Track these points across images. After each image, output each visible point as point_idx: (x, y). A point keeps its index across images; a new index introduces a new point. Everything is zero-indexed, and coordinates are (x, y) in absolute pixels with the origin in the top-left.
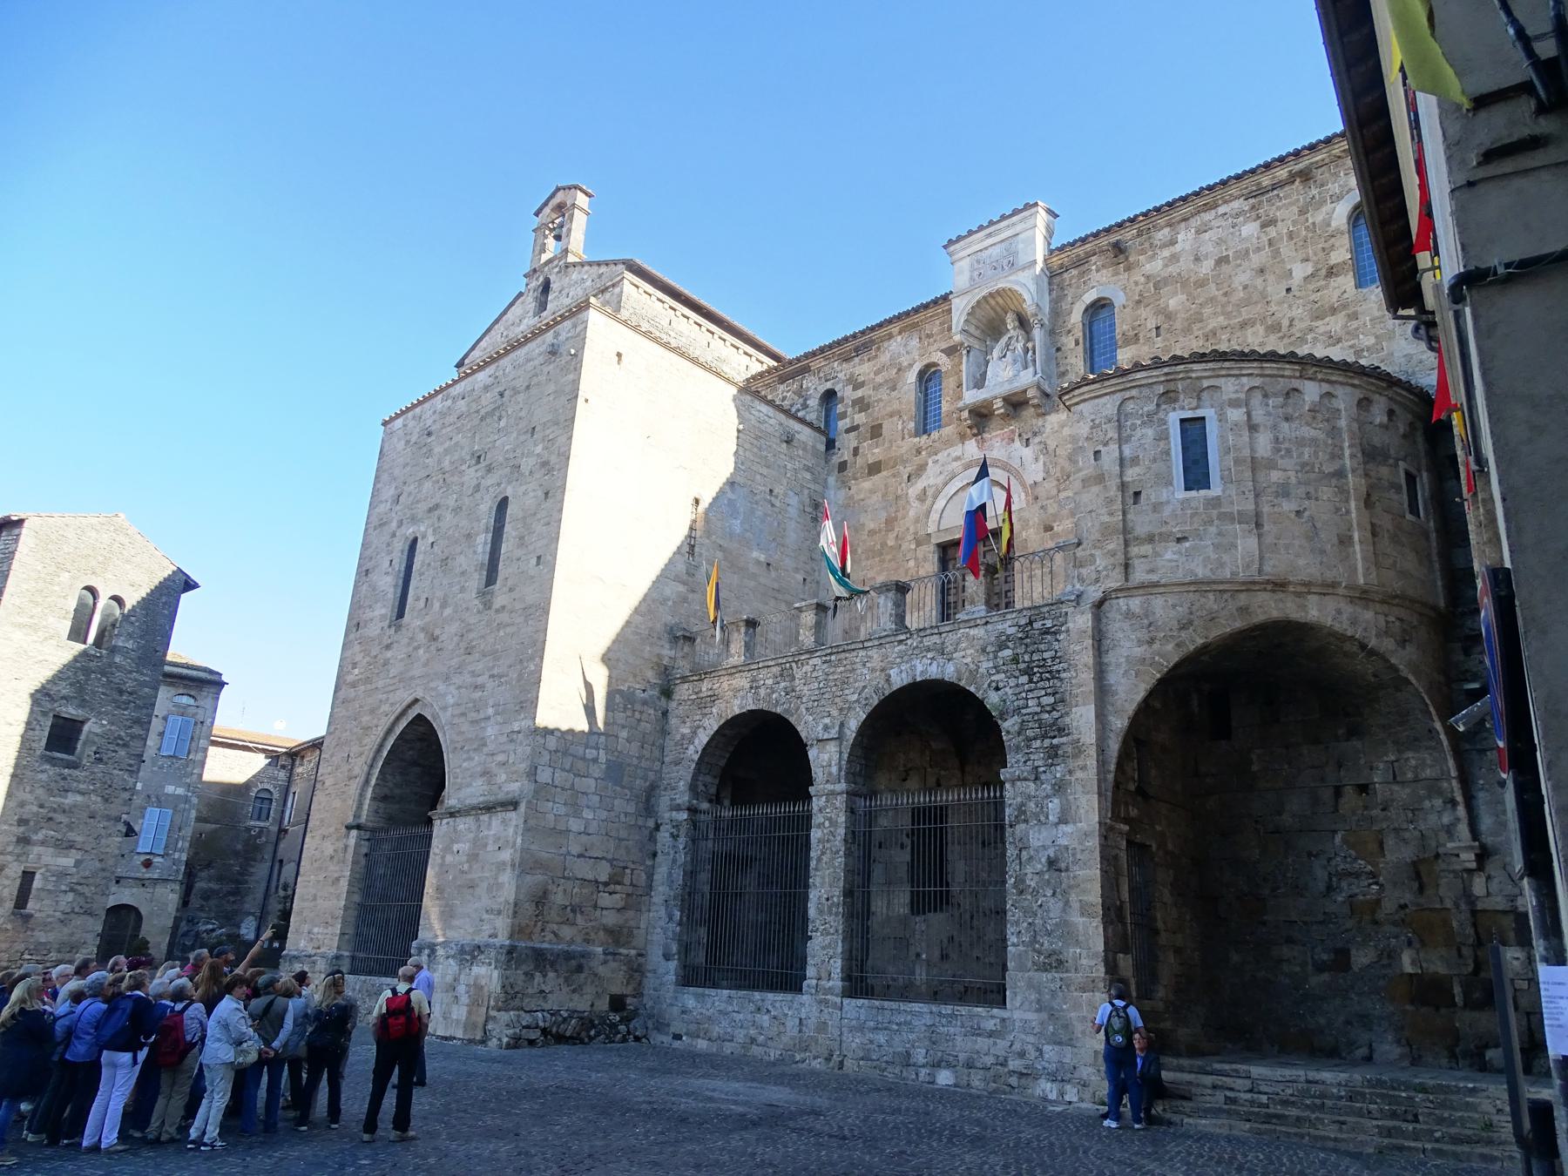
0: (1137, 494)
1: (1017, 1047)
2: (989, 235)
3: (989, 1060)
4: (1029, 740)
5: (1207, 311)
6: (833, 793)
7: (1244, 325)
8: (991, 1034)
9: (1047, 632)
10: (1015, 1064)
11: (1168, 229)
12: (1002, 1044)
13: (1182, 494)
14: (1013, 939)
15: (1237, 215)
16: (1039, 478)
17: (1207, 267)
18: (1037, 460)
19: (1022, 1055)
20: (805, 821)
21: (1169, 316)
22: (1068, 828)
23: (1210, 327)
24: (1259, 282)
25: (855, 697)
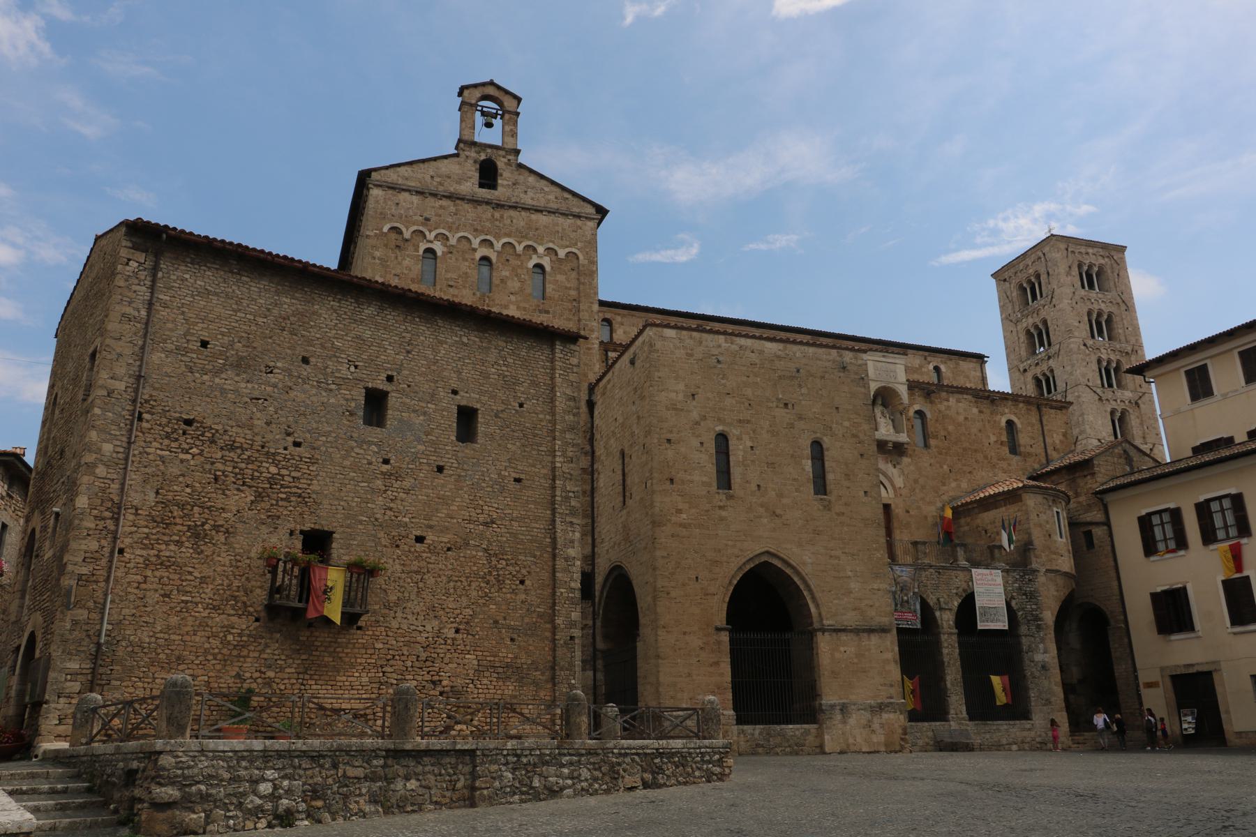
0: (1050, 535)
1: (1038, 733)
2: (884, 356)
3: (1029, 739)
4: (1029, 621)
5: (963, 438)
6: (951, 634)
7: (976, 451)
8: (1029, 729)
9: (1030, 580)
10: (1038, 739)
11: (945, 393)
12: (1033, 734)
13: (1060, 539)
14: (1033, 695)
15: (971, 402)
16: (902, 486)
17: (961, 418)
18: (900, 477)
19: (1040, 736)
20: (938, 644)
21: (949, 433)
22: (1048, 655)
23: (964, 446)
24: (980, 434)
25: (955, 591)
